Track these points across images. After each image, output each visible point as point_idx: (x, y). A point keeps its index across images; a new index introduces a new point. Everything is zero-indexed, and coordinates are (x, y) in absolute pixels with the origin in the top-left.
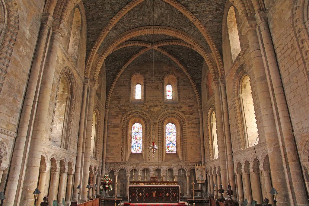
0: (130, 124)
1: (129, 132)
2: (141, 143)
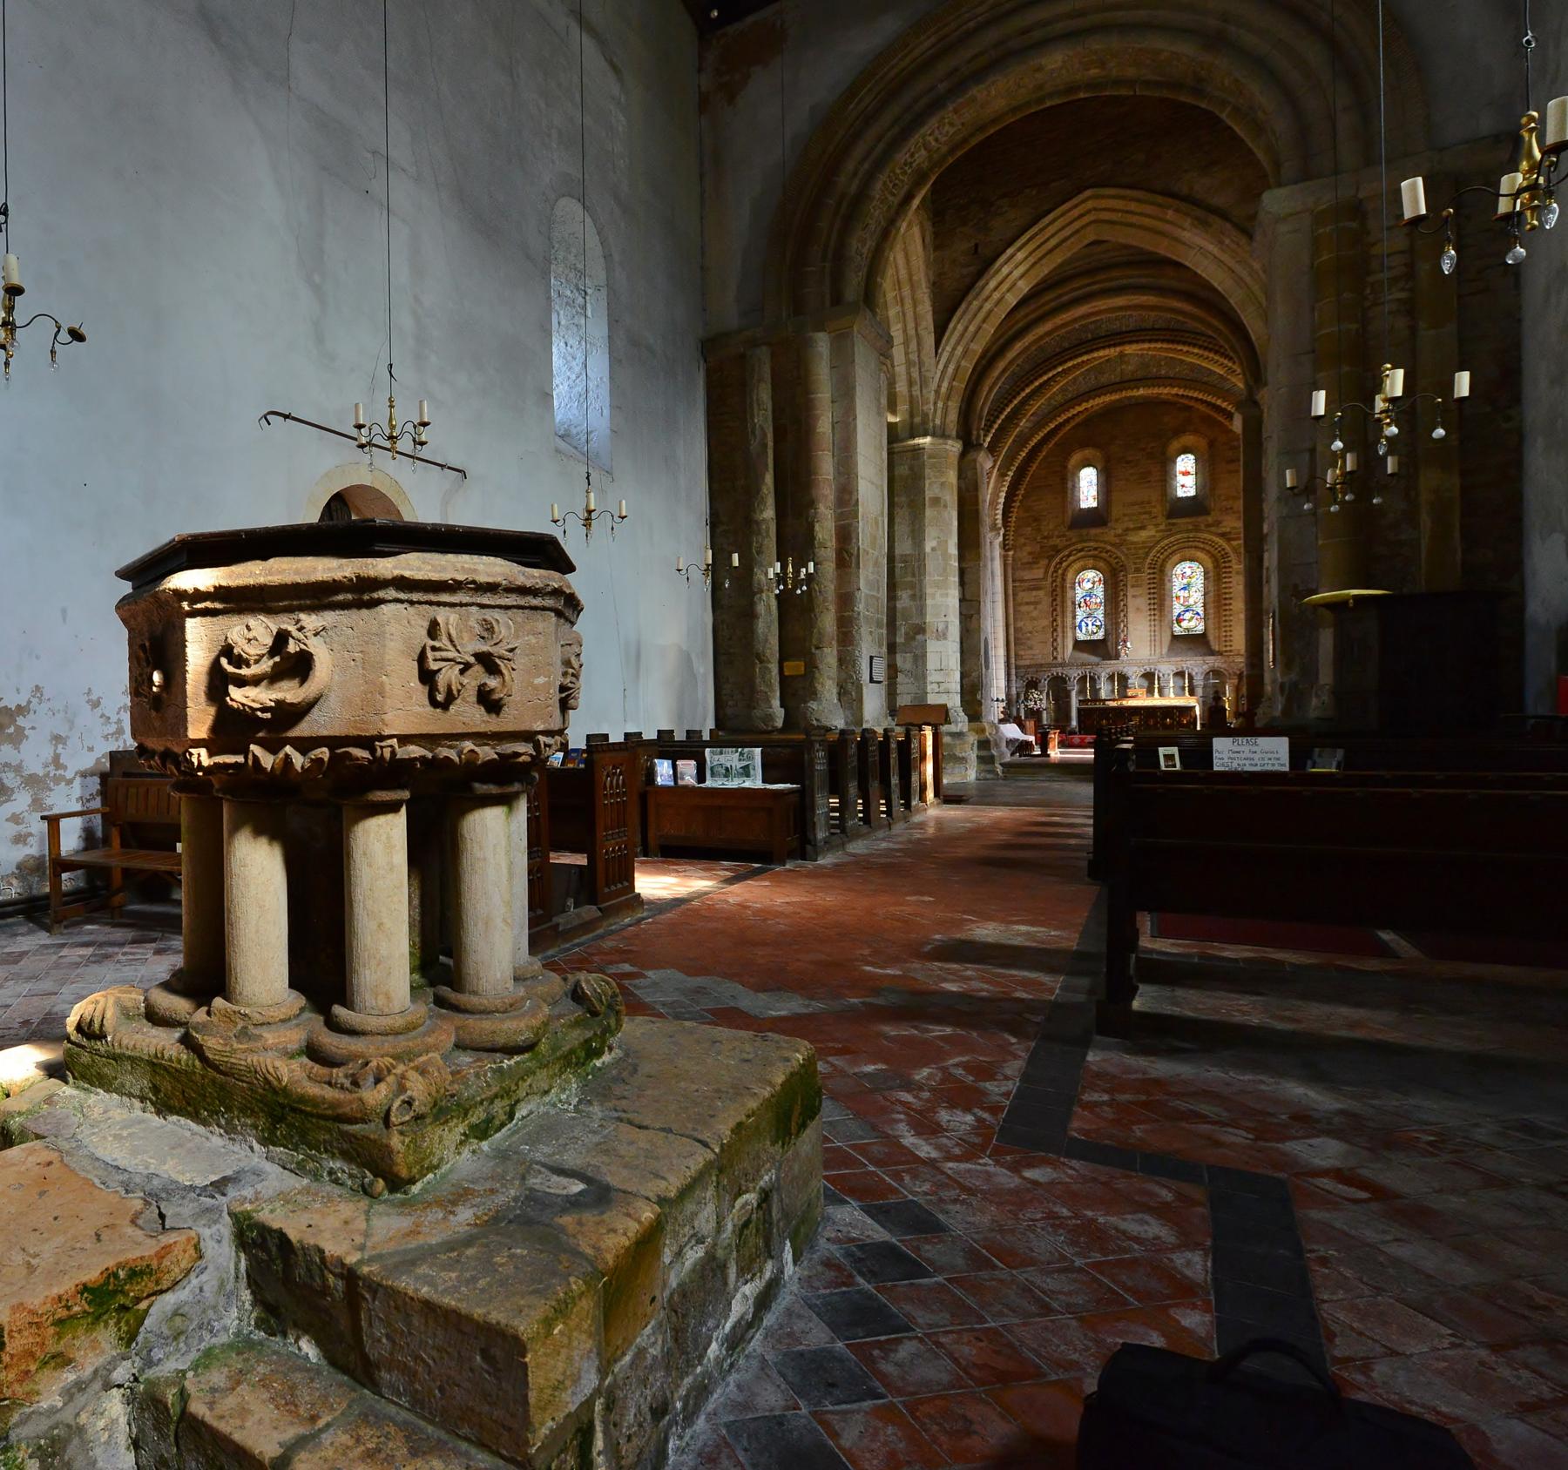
0: (1070, 575)
1: (1069, 594)
2: (1101, 617)
